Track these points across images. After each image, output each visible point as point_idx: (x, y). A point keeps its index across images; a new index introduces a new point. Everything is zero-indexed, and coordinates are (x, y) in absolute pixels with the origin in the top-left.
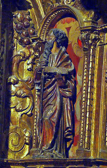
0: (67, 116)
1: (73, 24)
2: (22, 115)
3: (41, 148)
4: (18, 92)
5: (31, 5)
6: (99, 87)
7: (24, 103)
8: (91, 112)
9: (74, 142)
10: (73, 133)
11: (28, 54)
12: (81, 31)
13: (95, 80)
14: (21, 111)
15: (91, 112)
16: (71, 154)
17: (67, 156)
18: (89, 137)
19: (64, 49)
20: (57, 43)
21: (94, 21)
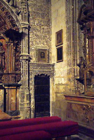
0: (3, 63)
1: (4, 41)
6: (11, 56)
8: (9, 62)
9: (5, 69)
10: (5, 67)
15: (9, 62)
16: (4, 72)
18: (9, 68)
21: (9, 40)
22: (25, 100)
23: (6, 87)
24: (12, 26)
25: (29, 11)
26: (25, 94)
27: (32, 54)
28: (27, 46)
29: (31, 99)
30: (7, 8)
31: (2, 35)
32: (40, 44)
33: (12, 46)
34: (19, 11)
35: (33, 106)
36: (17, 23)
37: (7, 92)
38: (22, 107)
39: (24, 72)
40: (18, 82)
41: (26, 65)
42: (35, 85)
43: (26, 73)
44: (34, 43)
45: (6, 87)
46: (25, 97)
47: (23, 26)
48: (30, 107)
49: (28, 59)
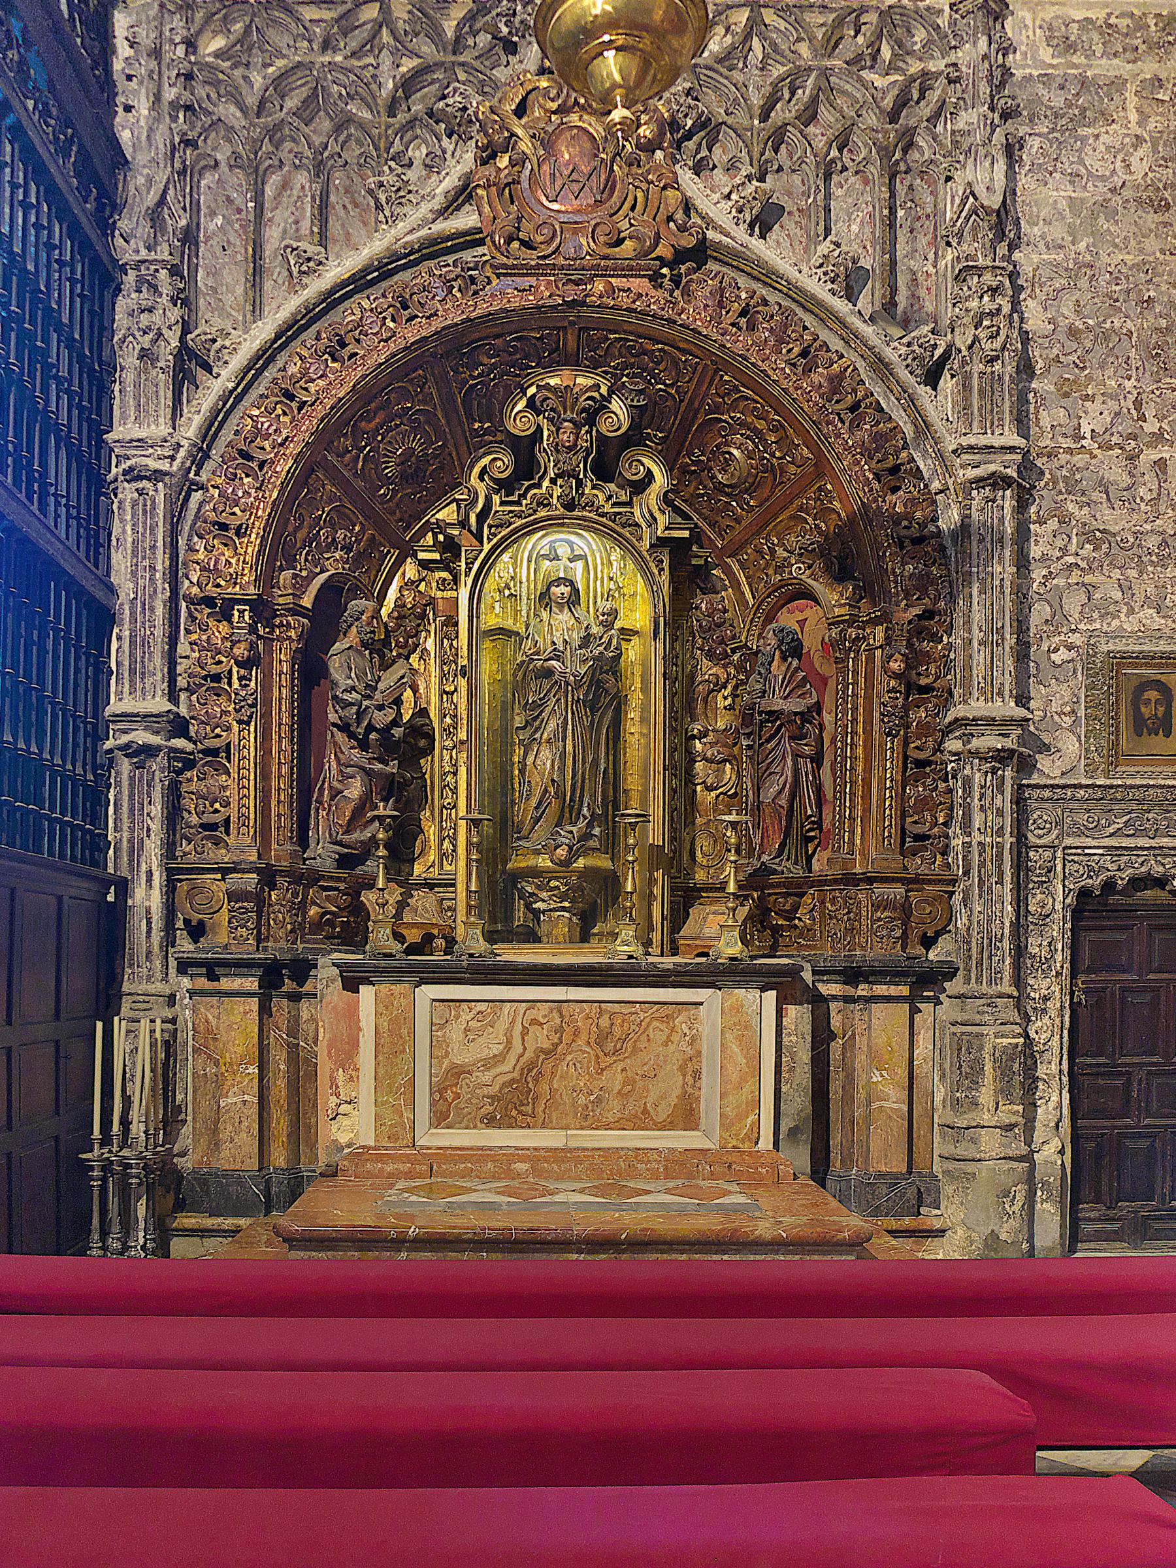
1: (812, 613)
2: (717, 797)
3: (759, 858)
4: (709, 754)
5: (727, 582)
6: (868, 732)
7: (720, 773)
10: (819, 823)
11: (723, 677)
12: (829, 625)
13: (861, 719)
14: (716, 789)
16: (816, 866)
17: (810, 872)
19: (795, 663)
20: (782, 652)
22: (986, 1095)
23: (830, 989)
24: (876, 485)
25: (1025, 338)
26: (988, 1048)
27: (1055, 707)
28: (1010, 640)
29: (1041, 1085)
30: (836, 344)
31: (797, 569)
32: (1131, 611)
33: (878, 653)
34: (938, 352)
35: (1055, 1144)
36: (917, 456)
37: (836, 1022)
38: (960, 1152)
39: (982, 865)
40: (928, 942)
41: (998, 801)
42: (1073, 976)
43: (1001, 875)
44: (1073, 604)
45: (830, 989)
46: (988, 1068)
47: (971, 473)
48: (1028, 1158)
49: (1012, 752)
